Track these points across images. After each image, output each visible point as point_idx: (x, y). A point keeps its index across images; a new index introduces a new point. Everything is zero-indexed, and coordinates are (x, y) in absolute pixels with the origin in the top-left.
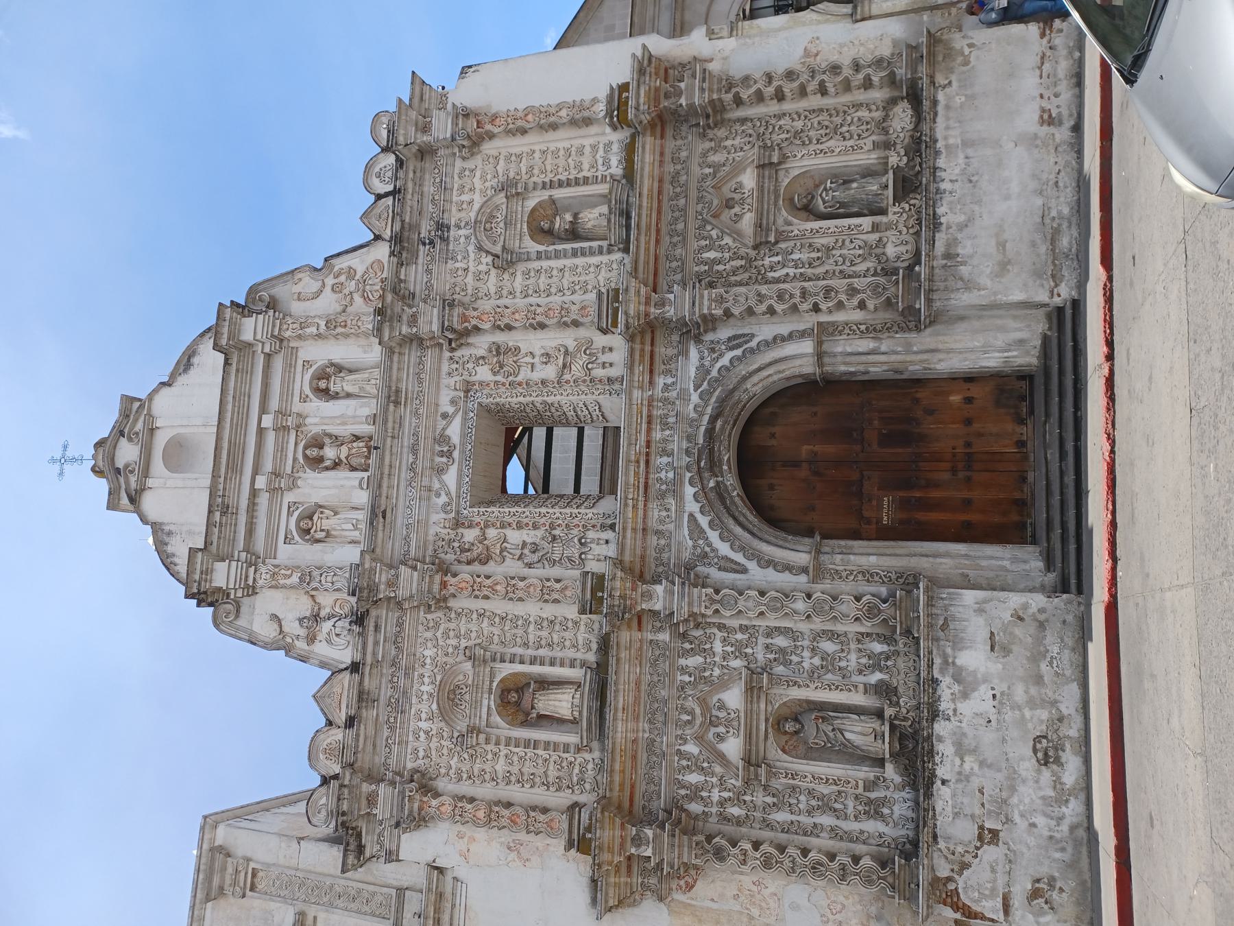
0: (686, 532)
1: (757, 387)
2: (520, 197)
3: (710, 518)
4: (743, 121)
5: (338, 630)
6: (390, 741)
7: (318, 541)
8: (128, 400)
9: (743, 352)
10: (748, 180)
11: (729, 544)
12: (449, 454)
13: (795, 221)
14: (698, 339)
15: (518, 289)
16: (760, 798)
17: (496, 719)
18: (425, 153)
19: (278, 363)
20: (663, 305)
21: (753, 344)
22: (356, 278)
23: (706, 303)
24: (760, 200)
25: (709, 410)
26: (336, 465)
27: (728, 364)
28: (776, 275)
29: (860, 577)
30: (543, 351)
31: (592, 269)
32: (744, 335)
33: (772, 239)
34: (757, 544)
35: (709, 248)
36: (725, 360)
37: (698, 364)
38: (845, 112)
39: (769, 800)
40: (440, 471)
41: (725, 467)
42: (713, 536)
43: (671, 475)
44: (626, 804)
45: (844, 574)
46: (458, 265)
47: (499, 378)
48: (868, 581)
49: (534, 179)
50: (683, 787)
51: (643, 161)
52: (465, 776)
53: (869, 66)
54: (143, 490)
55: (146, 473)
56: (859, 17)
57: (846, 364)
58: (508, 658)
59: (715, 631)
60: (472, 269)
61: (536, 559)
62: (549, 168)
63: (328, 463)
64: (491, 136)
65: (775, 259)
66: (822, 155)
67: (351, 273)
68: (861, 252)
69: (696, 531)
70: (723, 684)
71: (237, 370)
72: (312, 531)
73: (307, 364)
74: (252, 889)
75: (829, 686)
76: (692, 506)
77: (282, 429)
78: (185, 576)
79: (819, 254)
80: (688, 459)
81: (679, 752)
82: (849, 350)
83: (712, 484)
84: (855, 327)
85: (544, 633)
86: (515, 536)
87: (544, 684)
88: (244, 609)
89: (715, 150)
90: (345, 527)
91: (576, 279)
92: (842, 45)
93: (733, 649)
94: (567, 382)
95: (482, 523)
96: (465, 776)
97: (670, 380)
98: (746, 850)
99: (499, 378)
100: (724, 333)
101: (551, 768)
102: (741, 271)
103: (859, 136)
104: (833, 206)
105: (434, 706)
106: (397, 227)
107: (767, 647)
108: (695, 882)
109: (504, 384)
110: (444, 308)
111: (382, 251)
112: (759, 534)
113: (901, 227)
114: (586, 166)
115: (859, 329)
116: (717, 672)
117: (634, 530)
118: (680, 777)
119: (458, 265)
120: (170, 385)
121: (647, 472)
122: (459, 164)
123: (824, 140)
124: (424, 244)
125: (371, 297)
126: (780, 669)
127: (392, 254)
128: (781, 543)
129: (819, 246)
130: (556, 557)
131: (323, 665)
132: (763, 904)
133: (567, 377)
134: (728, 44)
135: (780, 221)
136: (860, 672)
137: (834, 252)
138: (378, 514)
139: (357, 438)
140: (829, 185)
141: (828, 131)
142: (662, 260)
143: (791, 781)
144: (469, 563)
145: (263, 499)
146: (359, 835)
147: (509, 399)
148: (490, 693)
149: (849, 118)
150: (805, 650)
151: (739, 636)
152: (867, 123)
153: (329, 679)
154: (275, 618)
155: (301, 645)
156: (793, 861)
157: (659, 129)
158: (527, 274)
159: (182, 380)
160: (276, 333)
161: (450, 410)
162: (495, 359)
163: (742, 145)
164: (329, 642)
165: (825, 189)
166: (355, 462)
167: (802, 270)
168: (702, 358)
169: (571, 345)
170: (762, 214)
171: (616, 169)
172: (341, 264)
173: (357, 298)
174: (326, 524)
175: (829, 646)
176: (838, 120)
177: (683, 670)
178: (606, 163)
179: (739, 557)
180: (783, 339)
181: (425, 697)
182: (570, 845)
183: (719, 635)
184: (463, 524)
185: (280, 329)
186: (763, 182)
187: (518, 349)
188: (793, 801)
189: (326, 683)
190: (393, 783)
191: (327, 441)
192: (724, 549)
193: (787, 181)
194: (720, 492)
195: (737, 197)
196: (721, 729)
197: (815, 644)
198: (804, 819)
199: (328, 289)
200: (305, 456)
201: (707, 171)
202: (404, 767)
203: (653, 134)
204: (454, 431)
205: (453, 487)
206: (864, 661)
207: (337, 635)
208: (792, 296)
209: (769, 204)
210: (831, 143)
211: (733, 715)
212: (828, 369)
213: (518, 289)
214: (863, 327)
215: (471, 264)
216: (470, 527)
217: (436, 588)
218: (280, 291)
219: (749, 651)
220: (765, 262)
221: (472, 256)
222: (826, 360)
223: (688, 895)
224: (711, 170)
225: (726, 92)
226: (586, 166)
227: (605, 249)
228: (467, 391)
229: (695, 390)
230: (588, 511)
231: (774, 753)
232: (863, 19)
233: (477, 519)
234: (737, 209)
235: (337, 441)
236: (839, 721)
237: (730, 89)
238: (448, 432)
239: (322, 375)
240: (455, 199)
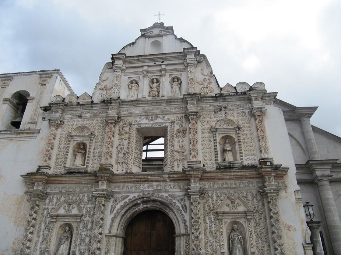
0: (124, 194)
1: (171, 215)
2: (235, 132)
3: (127, 202)
4: (263, 205)
5: (103, 96)
6: (72, 115)
7: (129, 86)
8: (171, 28)
9: (181, 210)
10: (241, 208)
11: (119, 208)
12: (152, 120)
13: (226, 225)
14: (185, 195)
15: (204, 135)
16: (48, 220)
17: (75, 143)
18: (250, 100)
19: (181, 67)
20: (194, 182)
21: (183, 213)
22: (208, 85)
23: (195, 196)
24: (235, 213)
25: (162, 200)
26: (151, 88)
27: (177, 205)
29: (107, 250)
30: (184, 145)
31: (210, 158)
32: (186, 210)
33: (219, 218)
34: (119, 217)
35: (217, 196)
36: (178, 204)
37: (177, 195)
38: (266, 241)
39: (47, 223)
40: (147, 118)
41: (145, 206)
42: (122, 203)
43: (142, 189)
44: (49, 182)
45: (108, 245)
46: (212, 115)
47: (175, 132)
48: (106, 252)
49: (242, 136)
50: (53, 198)
51: (246, 172)
52: (61, 136)
53: (281, 250)
54: (145, 37)
55: (150, 37)
56: (304, 245)
58: (91, 144)
59: (94, 205)
61: (119, 149)
62: (246, 140)
63: (151, 85)
64: (256, 120)
65: (213, 219)
66: (250, 234)
67: (210, 83)
68: (214, 249)
69: (124, 198)
70: (80, 209)
71: (179, 56)
72: (132, 84)
73: (181, 75)
74: (41, 85)
75: (76, 240)
76: (131, 196)
77: (161, 71)
78: (121, 53)
79: (214, 234)
80: (146, 194)
81: (62, 196)
82: (181, 245)
83: (139, 202)
84: (188, 247)
85: (97, 154)
86: (125, 142)
87: (85, 154)
88: (110, 70)
89: (252, 196)
90: (132, 93)
91: (207, 153)
92: (293, 239)
93: (88, 210)
94: (173, 154)
95: (130, 132)
96: (61, 136)
97: (172, 186)
98: (32, 216)
99: (175, 132)
100: (187, 203)
101: (62, 160)
102: (209, 207)
103: (257, 247)
104: (232, 239)
105: (80, 125)
106: (225, 95)
107: (88, 221)
108: (29, 202)
109: (173, 134)
110: (195, 112)
111: (217, 92)
112: (123, 218)
114: (247, 153)
115: (187, 249)
116: (82, 206)
117: (124, 179)
118: (55, 197)
119: (212, 115)
120: (176, 38)
122: (247, 111)
123: (256, 234)
125: (202, 90)
126: (82, 225)
127: (216, 94)
128: (121, 224)
129: (217, 234)
130: (119, 155)
131: (93, 93)
132: (22, 221)
133: (175, 153)
134: (293, 198)
135: (227, 220)
136: (79, 249)
137: (215, 239)
138: (133, 103)
139: (159, 92)
140: (240, 237)
141: (259, 235)
143: (51, 229)
144: (119, 130)
145: (140, 70)
147: (168, 136)
148: (82, 140)
149: (264, 243)
150: (87, 233)
152: (262, 250)
153: (89, 95)
154: (108, 78)
155: (99, 87)
156: (28, 229)
157: (259, 176)
158: (209, 137)
159: (178, 42)
160: (189, 65)
161: (166, 119)
162: (181, 130)
163: (254, 205)
164: (100, 94)
165: (238, 235)
166: (151, 93)
167: (208, 228)
169: (185, 154)
170: (229, 214)
171: (245, 163)
172: (213, 80)
173: (202, 86)
174: (133, 88)
175: (87, 240)
176: (263, 239)
177: (84, 196)
178: (248, 159)
179: (115, 211)
180: (185, 223)
181: (83, 122)
182: (40, 166)
183: (93, 206)
184: (130, 127)
185: (190, 66)
186: (240, 214)
187: (184, 137)
188: (46, 229)
189: (89, 95)
190: (61, 117)
192: (118, 207)
193: (241, 222)
194: (137, 205)
195: (235, 205)
196: (67, 208)
197: (88, 236)
198: (42, 233)
199: (204, 77)
200: (153, 79)
201: (245, 194)
202: (65, 119)
203: (257, 174)
204: (159, 120)
206: (82, 251)
207: (101, 96)
208: (196, 225)
209: (232, 216)
210: (254, 237)
211: (70, 211)
212: (177, 239)
213: (204, 135)
214: (188, 250)
215: (213, 119)
216: (129, 129)
217: (110, 121)
218: (204, 64)
219: (88, 215)
220: (211, 216)
221: (215, 119)
222: (179, 238)
223: (26, 200)
224: (245, 195)
225: (270, 198)
226: (247, 153)
227: (217, 161)
228: (171, 123)
229: (169, 195)
230: (133, 164)
231: (59, 224)
232: (304, 247)
233: (131, 131)
234: (231, 205)
235: (158, 87)
236: (67, 243)
237: (272, 200)
238: (159, 119)
239: (178, 79)
240: (235, 111)
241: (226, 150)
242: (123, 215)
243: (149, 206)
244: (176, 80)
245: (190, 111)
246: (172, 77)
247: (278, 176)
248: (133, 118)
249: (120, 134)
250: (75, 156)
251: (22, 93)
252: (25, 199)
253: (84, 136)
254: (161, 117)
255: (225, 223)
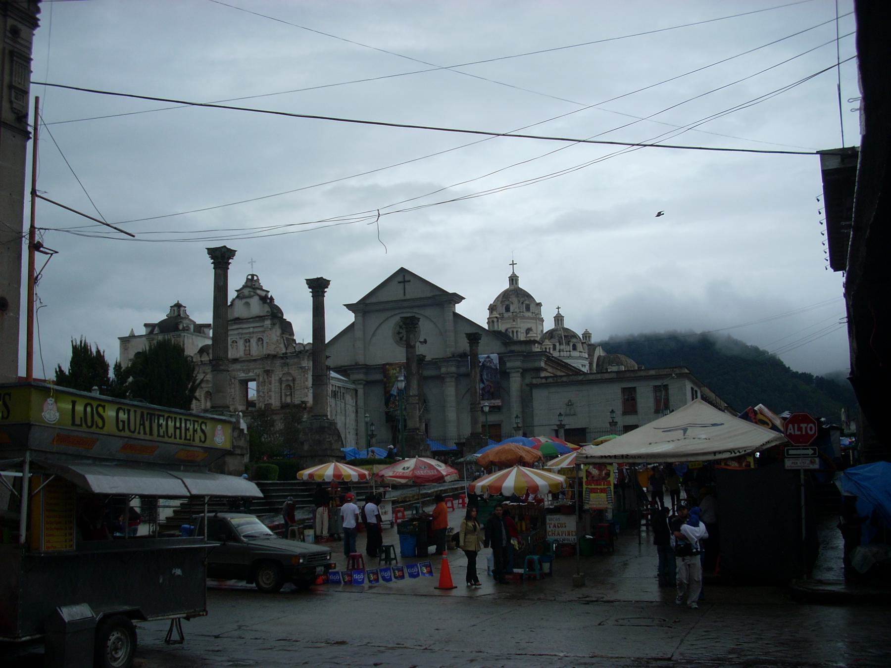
17: (205, 391)
26: (246, 346)
40: (244, 372)
73: (263, 336)
161: (255, 372)
205: (241, 376)
238: (251, 373)
244: (260, 340)
248: (236, 373)
250: (206, 400)
253: (209, 387)
254: (252, 371)
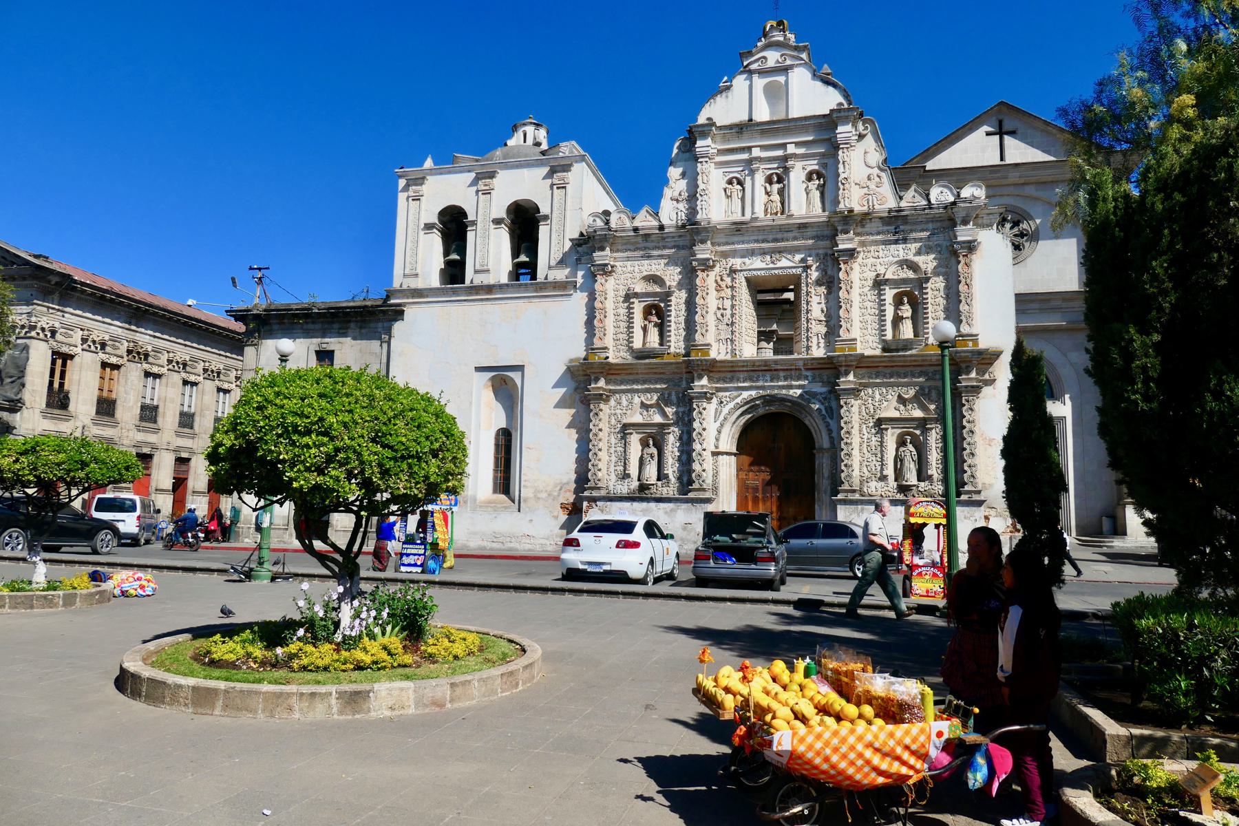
26: (767, 193)
28: (864, 430)
32: (833, 414)
42: (731, 405)
57: (819, 465)
60: (878, 261)
63: (769, 189)
86: (728, 303)
91: (869, 322)
113: (886, 488)
121: (762, 371)
124: (896, 228)
142: (876, 370)
144: (716, 281)
146: (586, 244)
151: (686, 419)
160: (841, 146)
168: (821, 394)
179: (722, 418)
183: (687, 410)
191: (781, 185)
192: (726, 410)
199: (870, 171)
200: (772, 174)
215: (881, 260)
241: (902, 318)
242: (734, 423)
243: (773, 409)
244: (815, 176)
245: (841, 247)
246: (806, 172)
247: (983, 362)
249: (719, 288)
251: (521, 205)
252: (577, 399)
255: (893, 435)
